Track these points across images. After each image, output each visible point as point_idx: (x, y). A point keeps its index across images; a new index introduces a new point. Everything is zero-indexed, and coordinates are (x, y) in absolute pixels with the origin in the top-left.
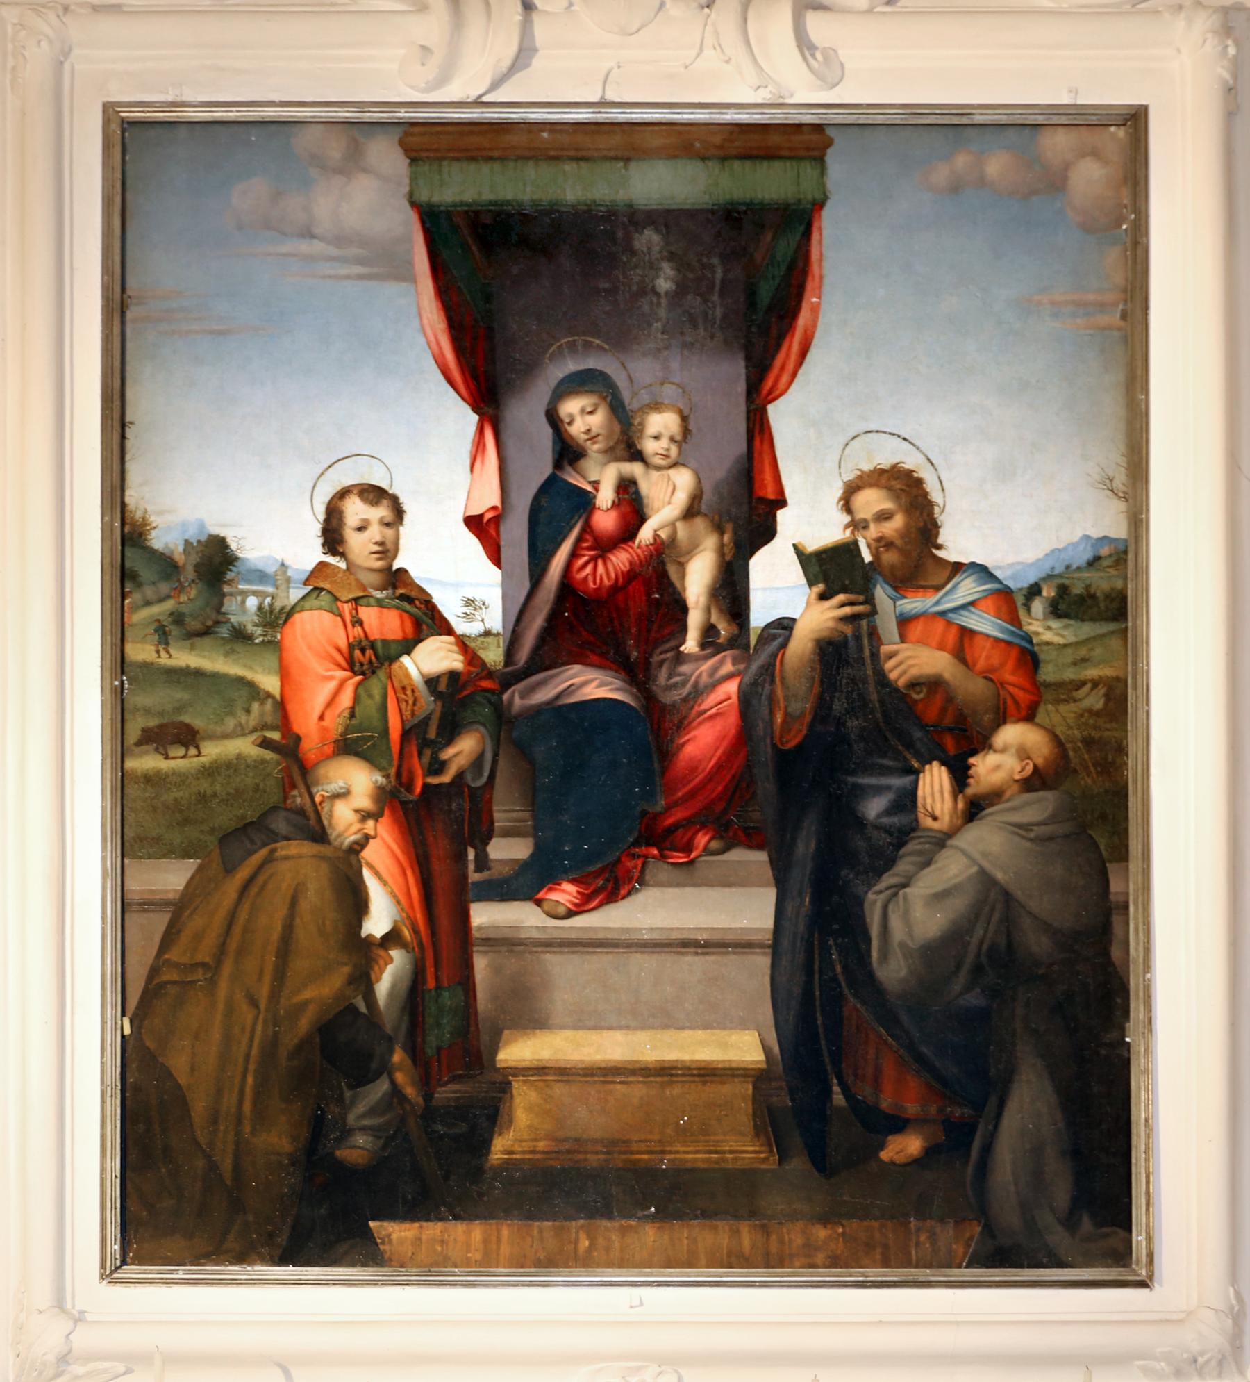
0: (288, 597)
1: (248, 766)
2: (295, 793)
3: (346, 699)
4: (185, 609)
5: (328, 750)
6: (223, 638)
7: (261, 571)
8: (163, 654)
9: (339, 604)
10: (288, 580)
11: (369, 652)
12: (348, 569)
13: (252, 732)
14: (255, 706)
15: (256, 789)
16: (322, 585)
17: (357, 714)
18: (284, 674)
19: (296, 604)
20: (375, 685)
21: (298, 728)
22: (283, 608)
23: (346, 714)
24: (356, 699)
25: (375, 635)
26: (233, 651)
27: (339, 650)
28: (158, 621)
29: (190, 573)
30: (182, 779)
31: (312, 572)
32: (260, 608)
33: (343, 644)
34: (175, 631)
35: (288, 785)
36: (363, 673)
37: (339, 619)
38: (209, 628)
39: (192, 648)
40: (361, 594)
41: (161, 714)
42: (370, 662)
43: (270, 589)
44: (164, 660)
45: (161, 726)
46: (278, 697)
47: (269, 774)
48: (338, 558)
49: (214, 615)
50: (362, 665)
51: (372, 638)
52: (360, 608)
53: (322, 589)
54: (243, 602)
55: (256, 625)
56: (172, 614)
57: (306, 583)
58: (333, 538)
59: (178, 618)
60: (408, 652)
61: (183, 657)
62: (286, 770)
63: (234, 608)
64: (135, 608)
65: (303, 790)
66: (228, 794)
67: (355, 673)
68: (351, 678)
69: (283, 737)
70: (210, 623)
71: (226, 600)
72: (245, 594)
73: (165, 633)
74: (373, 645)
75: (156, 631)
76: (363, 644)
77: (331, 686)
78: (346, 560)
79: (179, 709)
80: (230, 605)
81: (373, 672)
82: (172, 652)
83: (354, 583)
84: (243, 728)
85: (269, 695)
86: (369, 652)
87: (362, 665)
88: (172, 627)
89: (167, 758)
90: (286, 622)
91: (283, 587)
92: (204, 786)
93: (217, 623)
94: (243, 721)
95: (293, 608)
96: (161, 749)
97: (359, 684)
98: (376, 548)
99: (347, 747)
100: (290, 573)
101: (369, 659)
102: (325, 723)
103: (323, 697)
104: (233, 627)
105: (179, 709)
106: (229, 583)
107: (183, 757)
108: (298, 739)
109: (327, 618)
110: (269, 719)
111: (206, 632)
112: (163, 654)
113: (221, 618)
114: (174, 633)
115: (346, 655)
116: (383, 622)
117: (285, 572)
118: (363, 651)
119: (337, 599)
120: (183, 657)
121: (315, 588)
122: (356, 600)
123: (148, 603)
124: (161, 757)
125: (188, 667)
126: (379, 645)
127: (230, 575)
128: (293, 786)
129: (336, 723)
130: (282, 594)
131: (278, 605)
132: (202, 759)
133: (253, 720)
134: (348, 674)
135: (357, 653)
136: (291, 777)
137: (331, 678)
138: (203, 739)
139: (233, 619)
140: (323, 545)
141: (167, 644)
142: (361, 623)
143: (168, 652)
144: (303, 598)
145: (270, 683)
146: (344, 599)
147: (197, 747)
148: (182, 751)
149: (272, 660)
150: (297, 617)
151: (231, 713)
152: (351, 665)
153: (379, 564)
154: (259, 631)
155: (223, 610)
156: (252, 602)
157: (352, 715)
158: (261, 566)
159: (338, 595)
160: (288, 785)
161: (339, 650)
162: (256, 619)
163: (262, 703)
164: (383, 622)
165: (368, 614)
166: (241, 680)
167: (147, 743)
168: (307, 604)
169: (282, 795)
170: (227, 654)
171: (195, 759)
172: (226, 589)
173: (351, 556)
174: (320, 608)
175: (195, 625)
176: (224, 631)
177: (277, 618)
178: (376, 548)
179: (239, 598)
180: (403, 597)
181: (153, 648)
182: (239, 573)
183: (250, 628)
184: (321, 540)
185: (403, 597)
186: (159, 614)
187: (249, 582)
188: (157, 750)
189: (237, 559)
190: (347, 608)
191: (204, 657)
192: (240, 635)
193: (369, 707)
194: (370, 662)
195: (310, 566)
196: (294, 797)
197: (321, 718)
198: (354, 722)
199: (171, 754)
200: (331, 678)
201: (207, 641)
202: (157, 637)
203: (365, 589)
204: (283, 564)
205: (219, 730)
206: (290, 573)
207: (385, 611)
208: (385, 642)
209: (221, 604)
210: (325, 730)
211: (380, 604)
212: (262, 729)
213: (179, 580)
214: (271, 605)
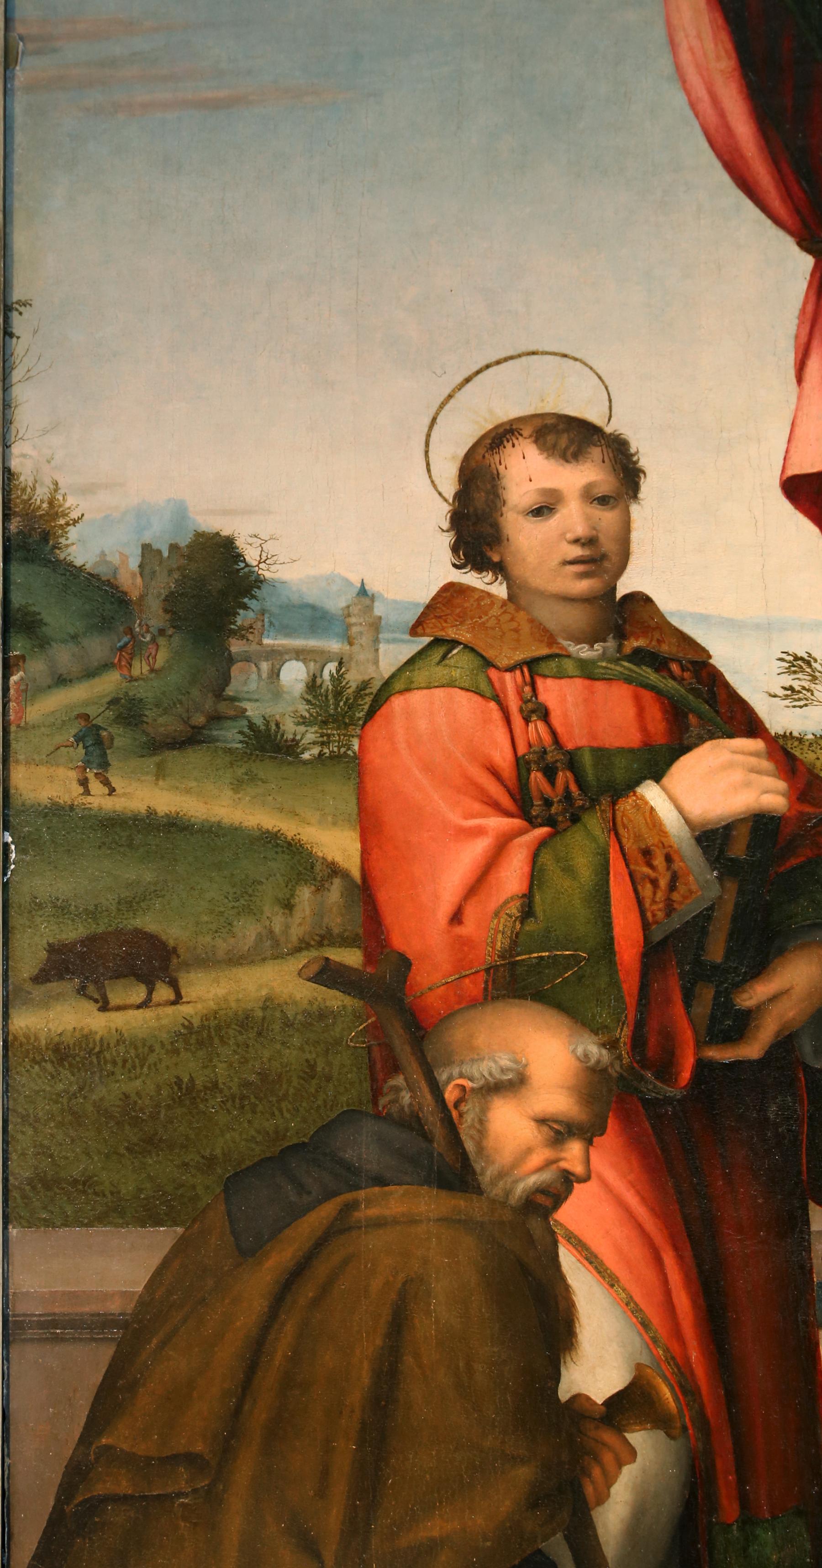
0: (376, 662)
1: (288, 1024)
2: (399, 1080)
3: (512, 877)
4: (141, 691)
5: (473, 987)
6: (230, 751)
7: (313, 608)
8: (95, 786)
9: (493, 674)
10: (376, 626)
11: (563, 777)
12: (511, 597)
13: (298, 950)
14: (305, 894)
15: (310, 1071)
16: (452, 633)
17: (538, 908)
18: (369, 825)
19: (393, 676)
20: (581, 847)
21: (398, 942)
22: (365, 685)
23: (514, 909)
24: (535, 876)
25: (576, 737)
26: (253, 778)
27: (494, 772)
28: (86, 717)
29: (154, 615)
30: (137, 1053)
31: (430, 608)
32: (313, 686)
33: (503, 757)
34: (121, 737)
35: (382, 1065)
36: (551, 822)
37: (493, 705)
38: (197, 729)
39: (161, 773)
40: (544, 651)
41: (93, 914)
42: (568, 796)
43: (335, 646)
44: (99, 799)
45: (90, 941)
46: (356, 873)
47: (338, 1042)
48: (489, 577)
49: (209, 704)
50: (548, 803)
51: (570, 746)
52: (540, 682)
53: (454, 643)
54: (275, 674)
55: (303, 721)
56: (114, 702)
57: (416, 629)
58: (475, 528)
59: (128, 711)
60: (657, 773)
61: (140, 792)
62: (377, 1030)
63: (253, 686)
64: (32, 691)
65: (417, 1076)
66: (246, 1084)
67: (532, 822)
68: (521, 832)
69: (369, 959)
70: (199, 719)
71: (235, 671)
72: (278, 657)
73: (99, 742)
74: (572, 761)
75: (79, 738)
76: (549, 758)
77: (479, 847)
78: (507, 578)
79: (130, 905)
80: (246, 681)
81: (575, 819)
82: (115, 782)
83: (526, 628)
84: (276, 944)
85: (335, 870)
86: (563, 777)
87: (548, 803)
88: (115, 730)
89: (105, 1007)
90: (371, 714)
91: (365, 640)
92: (190, 1066)
93: (216, 718)
94: (277, 929)
95: (387, 683)
96: (91, 989)
97: (542, 843)
98: (577, 552)
99: (518, 979)
100: (379, 609)
101: (563, 793)
102: (468, 928)
103: (460, 868)
104: (251, 726)
105: (130, 905)
106: (242, 633)
107: (139, 1007)
108: (404, 963)
109: (465, 704)
110: (336, 922)
111: (191, 738)
112: (95, 786)
113: (223, 708)
114: (117, 742)
115: (512, 782)
116: (592, 711)
117: (369, 608)
118: (550, 773)
119: (488, 663)
120: (140, 792)
121: (437, 642)
122: (532, 665)
123: (62, 681)
124: (92, 1007)
125: (151, 813)
126: (587, 760)
127: (243, 618)
128: (395, 1068)
129: (489, 928)
130: (362, 655)
131: (353, 678)
132: (185, 1010)
133: (299, 925)
134: (517, 822)
135: (537, 777)
136: (388, 1047)
137: (479, 832)
138: (187, 966)
139: (253, 711)
140: (455, 549)
141: (105, 765)
142: (545, 715)
143: (106, 783)
144: (411, 662)
145: (339, 845)
146: (504, 662)
147: (174, 985)
148: (139, 993)
149: (341, 795)
150: (397, 703)
151: (250, 911)
152: (522, 804)
153: (583, 586)
154: (311, 735)
155: (230, 691)
156: (294, 674)
157: (528, 912)
158: (312, 596)
159: (490, 654)
160: (382, 1065)
161: (494, 772)
162: (303, 709)
163: (320, 888)
164: (592, 711)
165: (560, 695)
166: (271, 840)
167: (61, 978)
168: (420, 676)
169: (367, 1085)
170: (238, 785)
171: (170, 1010)
172: (236, 646)
173: (517, 571)
174: (450, 684)
175: (165, 724)
176: (231, 735)
177: (351, 707)
178: (577, 552)
179: (265, 666)
180: (638, 656)
181: (73, 775)
182: (263, 612)
183: (290, 728)
184: (447, 539)
185: (638, 656)
186: (86, 703)
187: (287, 631)
188: (82, 991)
189: (259, 582)
190: (510, 682)
191: (188, 791)
192: (269, 745)
193: (567, 893)
194: (568, 796)
195: (425, 594)
196: (397, 1089)
197: (457, 918)
198: (531, 926)
199: (115, 999)
200: (479, 832)
201: (194, 757)
202: (81, 751)
203: (551, 640)
204: (363, 592)
205: (222, 946)
206: (379, 609)
207: (599, 686)
208: (601, 754)
209: (226, 679)
210: (464, 943)
211: (588, 671)
212: (320, 944)
213: (130, 631)
214: (337, 679)
